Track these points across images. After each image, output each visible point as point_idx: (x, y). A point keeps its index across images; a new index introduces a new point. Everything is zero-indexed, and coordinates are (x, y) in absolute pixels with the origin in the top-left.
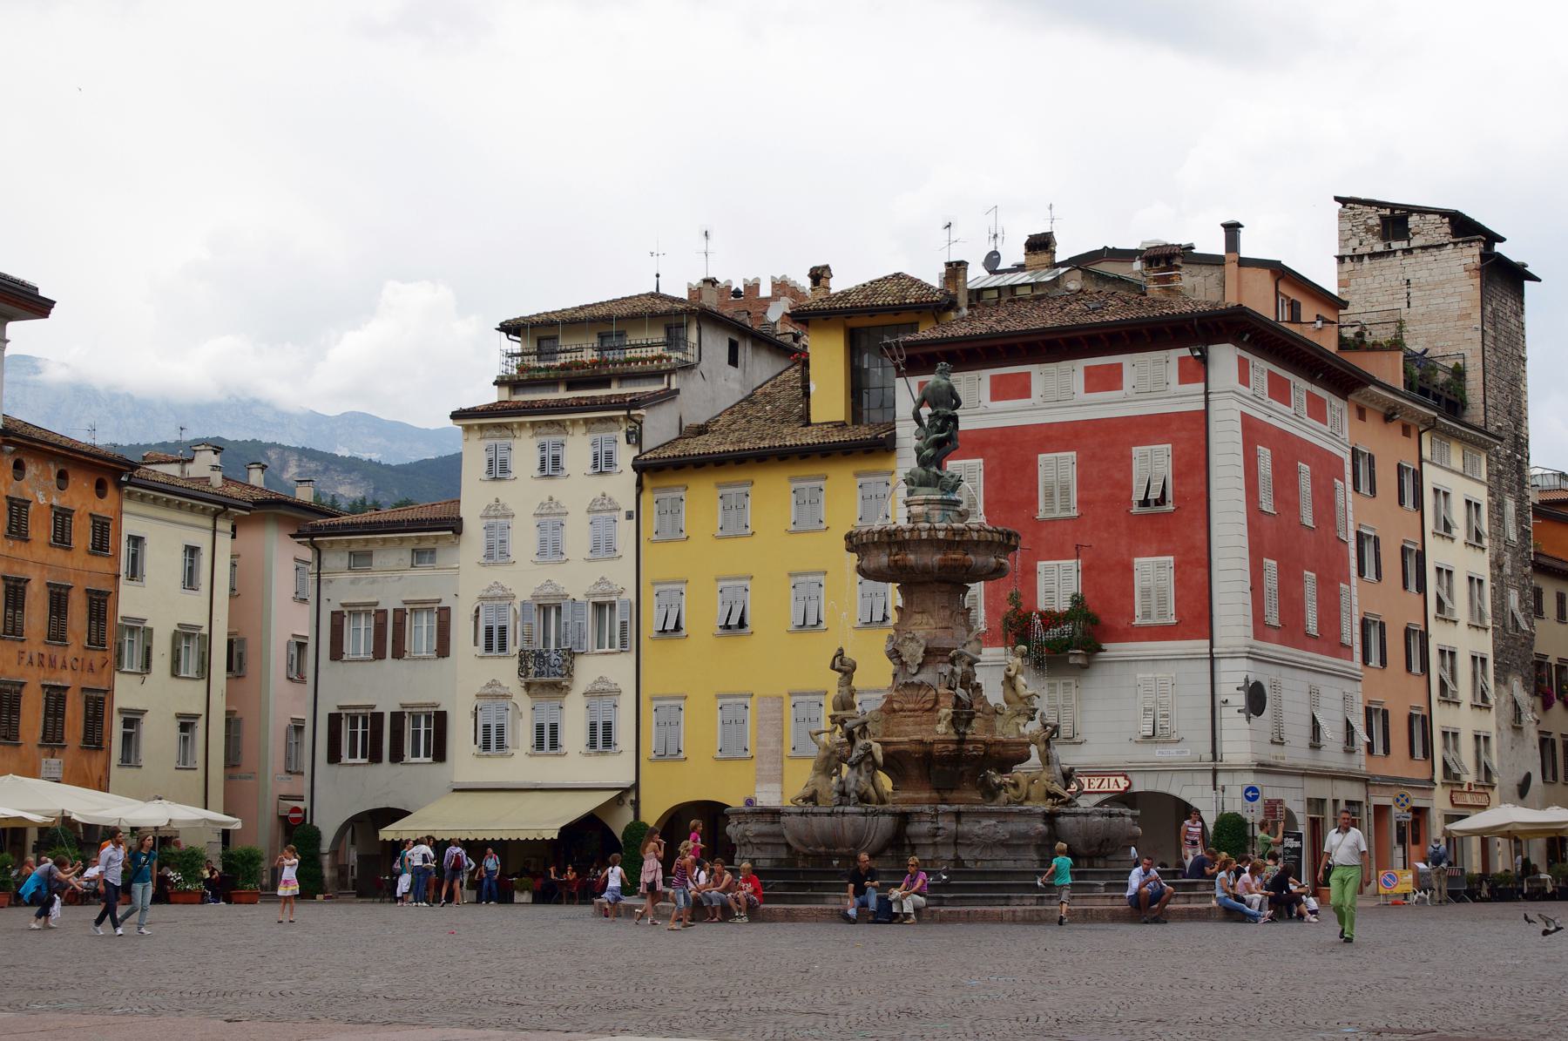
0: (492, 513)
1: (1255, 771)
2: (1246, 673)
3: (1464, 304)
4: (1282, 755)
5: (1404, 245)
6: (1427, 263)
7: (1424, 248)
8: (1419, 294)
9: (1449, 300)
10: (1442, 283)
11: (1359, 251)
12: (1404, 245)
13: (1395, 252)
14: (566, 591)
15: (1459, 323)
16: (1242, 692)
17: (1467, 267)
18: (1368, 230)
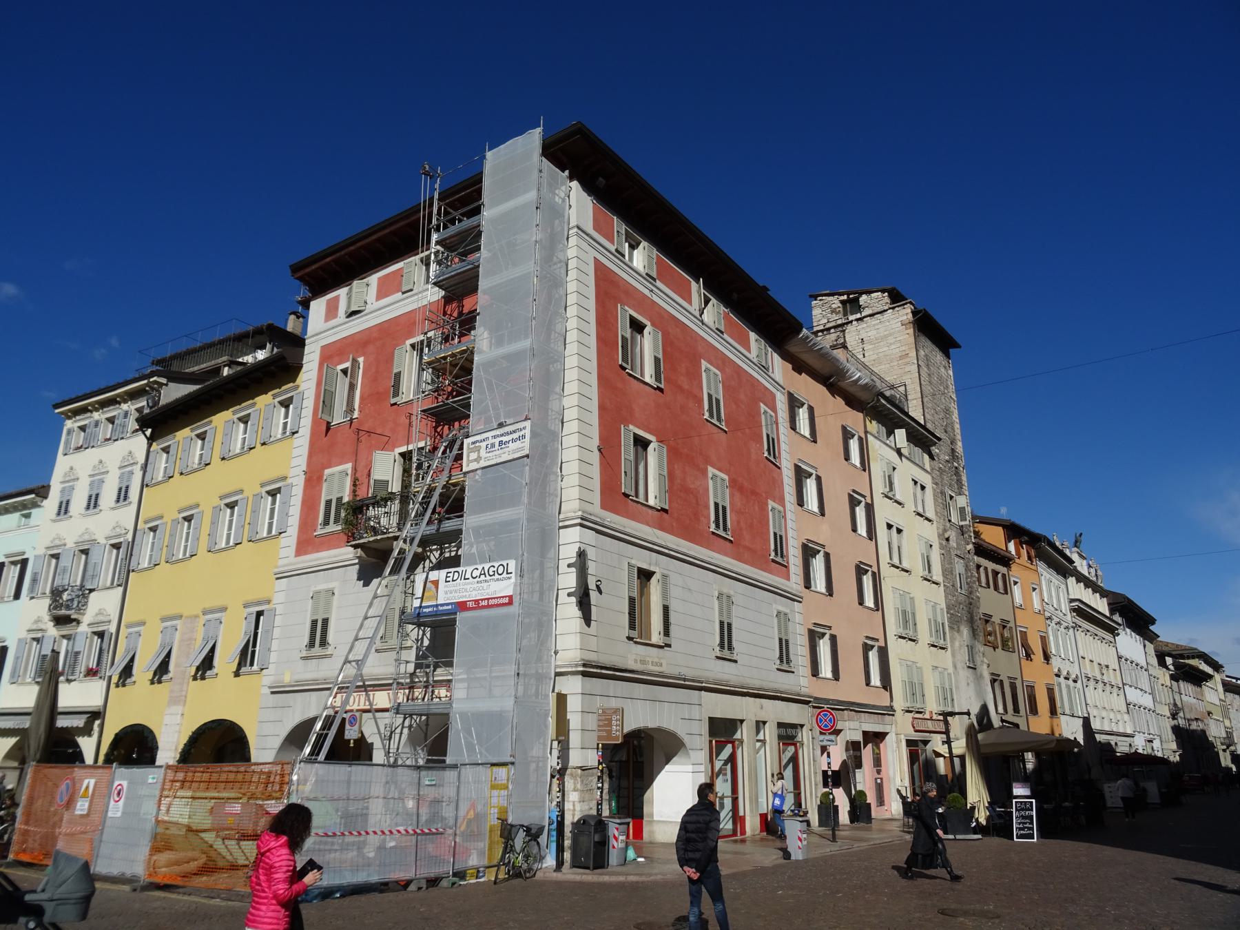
0: (67, 479)
1: (584, 674)
2: (578, 545)
3: (903, 348)
4: (656, 660)
5: (858, 316)
6: (874, 325)
7: (871, 315)
8: (871, 347)
9: (893, 347)
10: (886, 336)
11: (828, 325)
12: (858, 316)
13: (851, 322)
14: (96, 537)
15: (900, 362)
16: (573, 569)
17: (903, 323)
18: (834, 311)
